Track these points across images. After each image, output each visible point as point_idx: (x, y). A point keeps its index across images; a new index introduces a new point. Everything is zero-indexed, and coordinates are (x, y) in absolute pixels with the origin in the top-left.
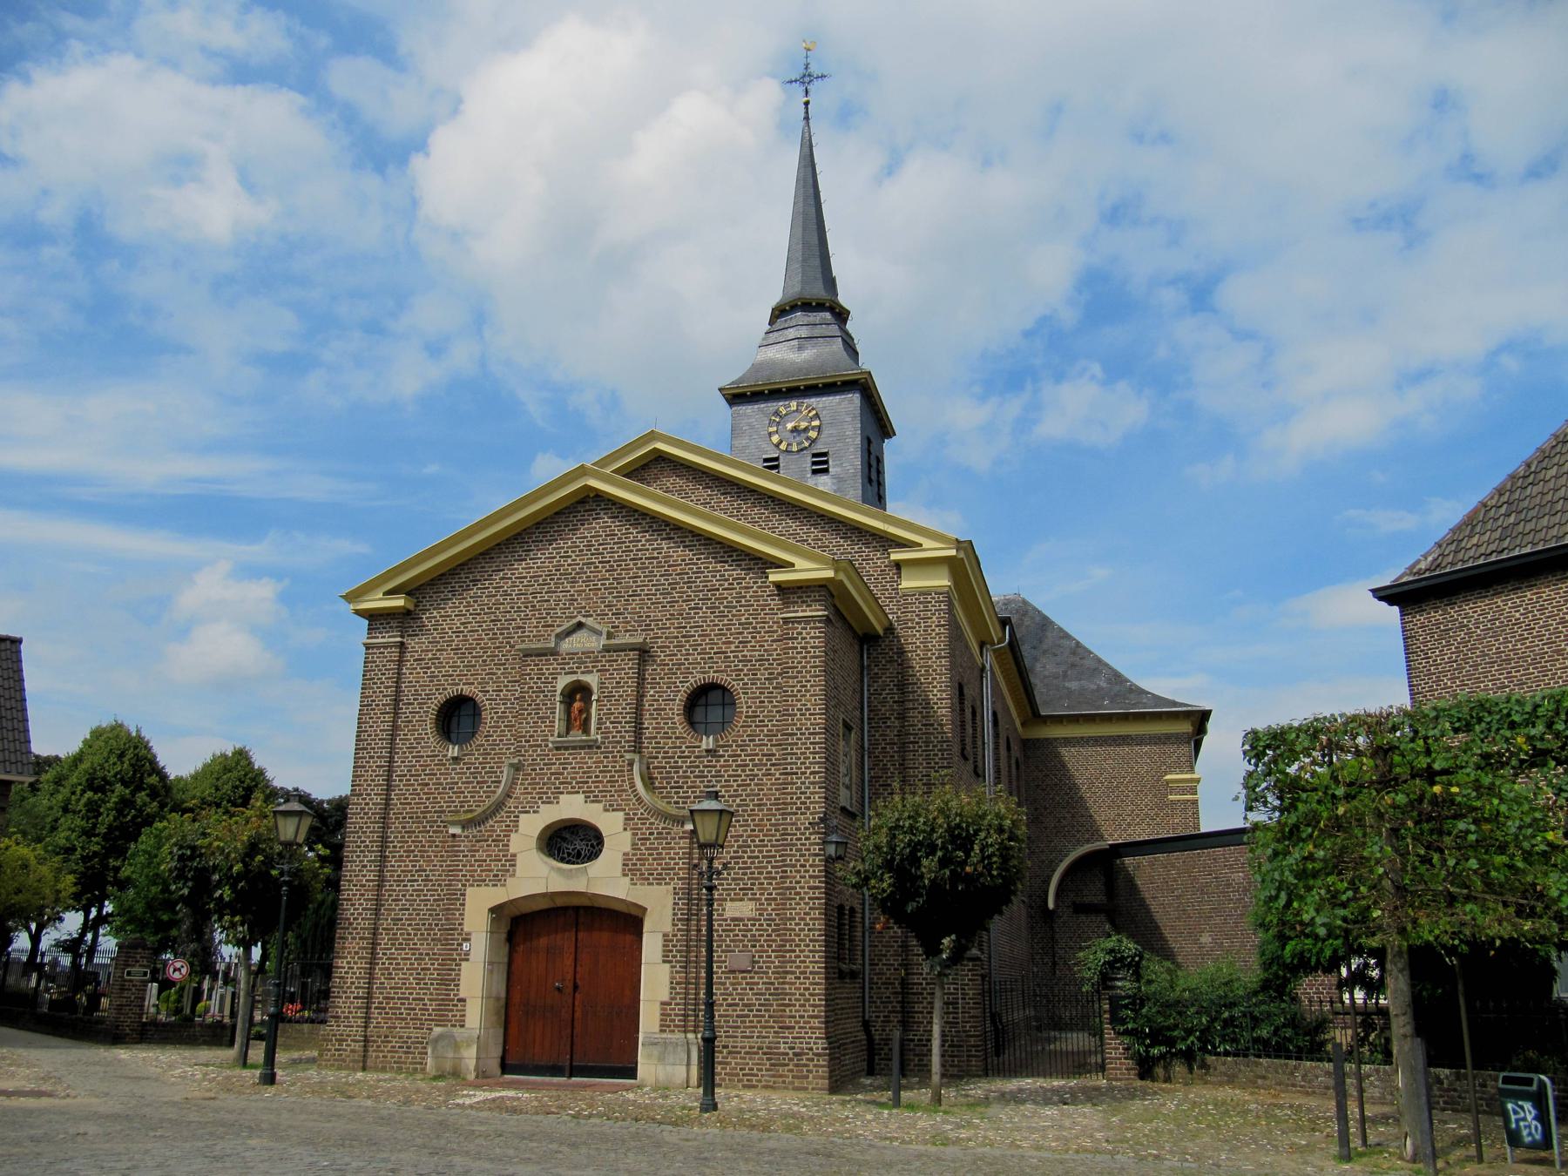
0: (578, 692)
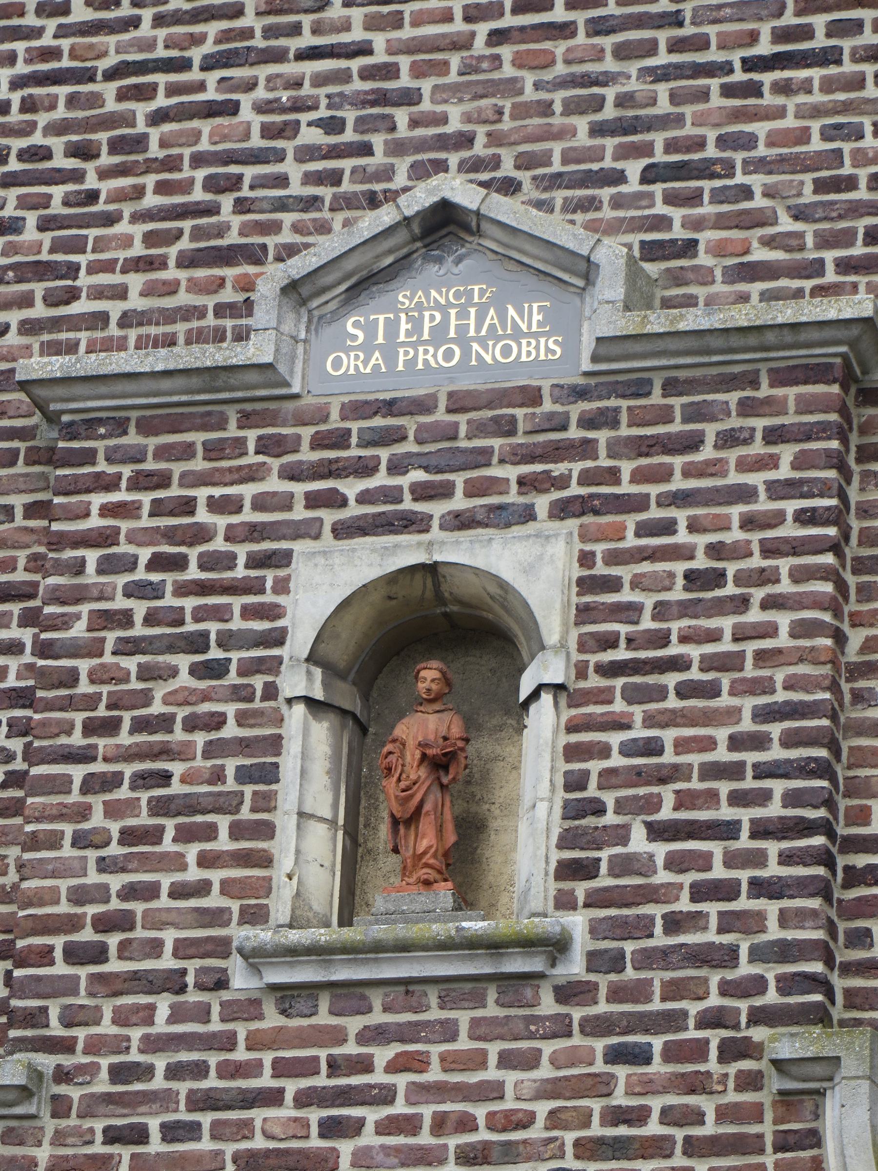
0: (433, 640)
